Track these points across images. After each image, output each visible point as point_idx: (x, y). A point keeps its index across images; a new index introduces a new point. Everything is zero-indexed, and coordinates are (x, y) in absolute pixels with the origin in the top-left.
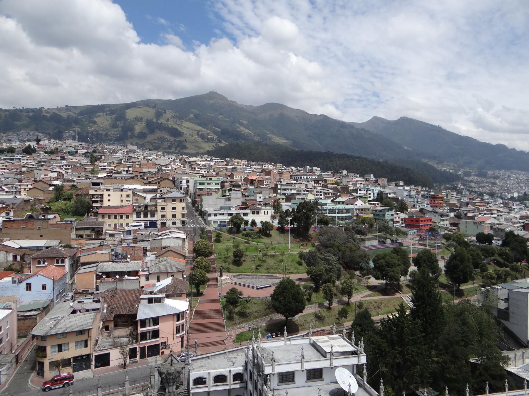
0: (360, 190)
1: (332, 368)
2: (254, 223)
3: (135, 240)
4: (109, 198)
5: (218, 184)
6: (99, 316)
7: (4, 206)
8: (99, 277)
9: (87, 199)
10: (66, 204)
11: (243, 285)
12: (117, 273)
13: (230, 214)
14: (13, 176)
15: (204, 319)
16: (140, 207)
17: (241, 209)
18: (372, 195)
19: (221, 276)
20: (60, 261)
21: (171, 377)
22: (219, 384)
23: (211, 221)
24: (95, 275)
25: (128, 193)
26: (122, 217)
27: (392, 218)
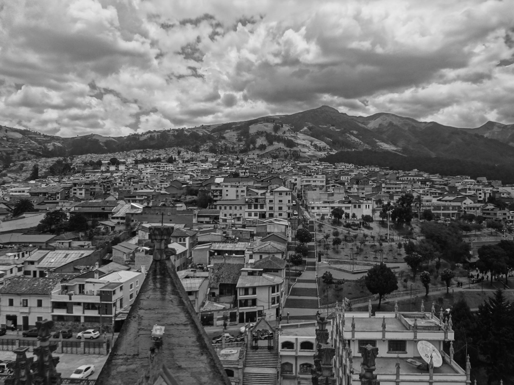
0: (470, 189)
1: (416, 341)
2: (354, 216)
3: (244, 226)
5: (323, 181)
6: (207, 282)
8: (211, 254)
11: (340, 270)
12: (226, 251)
13: (332, 208)
15: (300, 296)
17: (343, 202)
18: (483, 195)
19: (320, 260)
20: (182, 239)
22: (306, 350)
23: (314, 213)
25: (242, 189)
27: (504, 217)
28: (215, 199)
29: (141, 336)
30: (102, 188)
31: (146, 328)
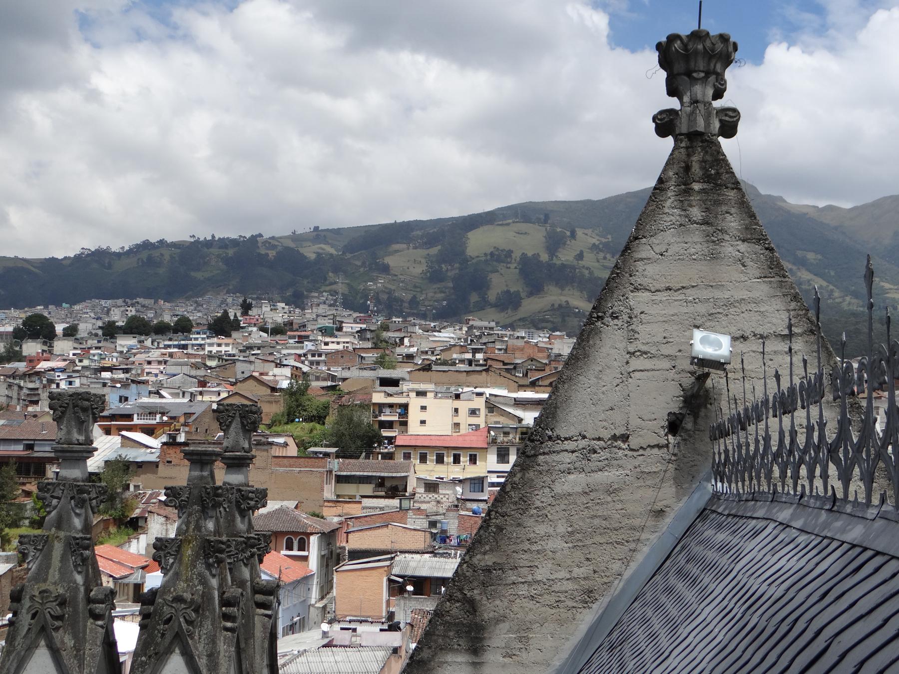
4: (423, 416)
7: (165, 418)
9: (367, 418)
10: (311, 431)
14: (186, 369)
16: (506, 434)
21: (700, 47)
24: (385, 579)
26: (457, 460)
28: (385, 433)
29: (637, 375)
30: (15, 396)
31: (653, 351)
